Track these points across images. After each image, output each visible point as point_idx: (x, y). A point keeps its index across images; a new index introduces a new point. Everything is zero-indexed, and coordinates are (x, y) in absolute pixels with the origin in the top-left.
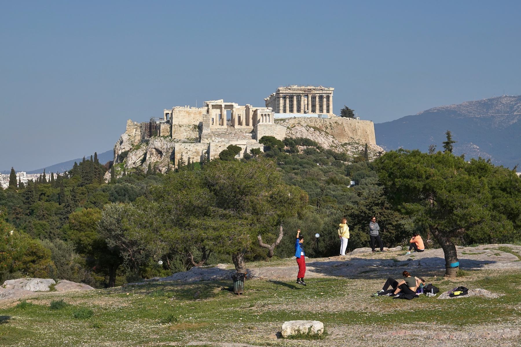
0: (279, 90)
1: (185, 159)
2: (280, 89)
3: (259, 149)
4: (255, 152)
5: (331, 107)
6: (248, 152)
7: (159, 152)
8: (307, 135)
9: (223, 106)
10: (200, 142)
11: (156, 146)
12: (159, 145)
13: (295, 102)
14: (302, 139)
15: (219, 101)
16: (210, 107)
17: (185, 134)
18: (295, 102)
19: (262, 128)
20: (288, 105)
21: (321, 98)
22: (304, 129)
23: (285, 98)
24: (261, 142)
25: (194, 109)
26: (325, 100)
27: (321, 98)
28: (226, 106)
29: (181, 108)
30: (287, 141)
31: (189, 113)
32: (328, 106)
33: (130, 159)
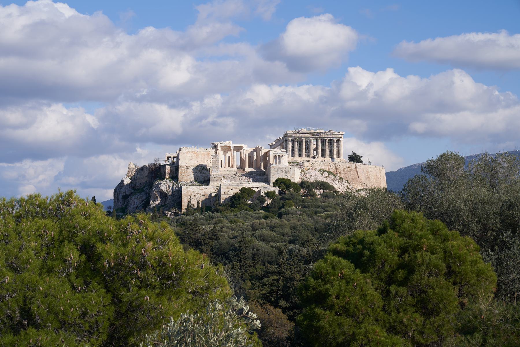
0: (287, 134)
2: (288, 132)
3: (274, 192)
5: (342, 152)
6: (262, 194)
7: (163, 195)
8: (321, 178)
9: (232, 148)
10: (208, 185)
12: (165, 187)
13: (304, 147)
14: (318, 182)
15: (228, 142)
16: (219, 148)
18: (304, 147)
19: (276, 170)
21: (331, 142)
22: (318, 174)
23: (293, 141)
24: (275, 185)
27: (331, 142)
29: (187, 149)
30: (303, 184)
33: (132, 202)
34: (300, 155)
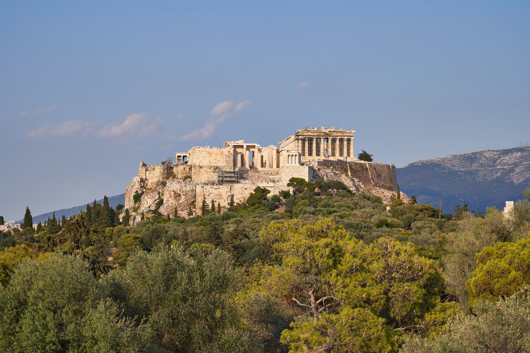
1: (209, 202)
3: (289, 191)
4: (286, 194)
5: (352, 151)
7: (177, 196)
11: (175, 189)
13: (314, 145)
17: (206, 175)
18: (314, 145)
19: (289, 169)
20: (307, 148)
21: (341, 140)
25: (215, 150)
26: (345, 142)
27: (341, 140)
28: (248, 148)
31: (210, 154)
32: (348, 150)
34: (310, 154)
